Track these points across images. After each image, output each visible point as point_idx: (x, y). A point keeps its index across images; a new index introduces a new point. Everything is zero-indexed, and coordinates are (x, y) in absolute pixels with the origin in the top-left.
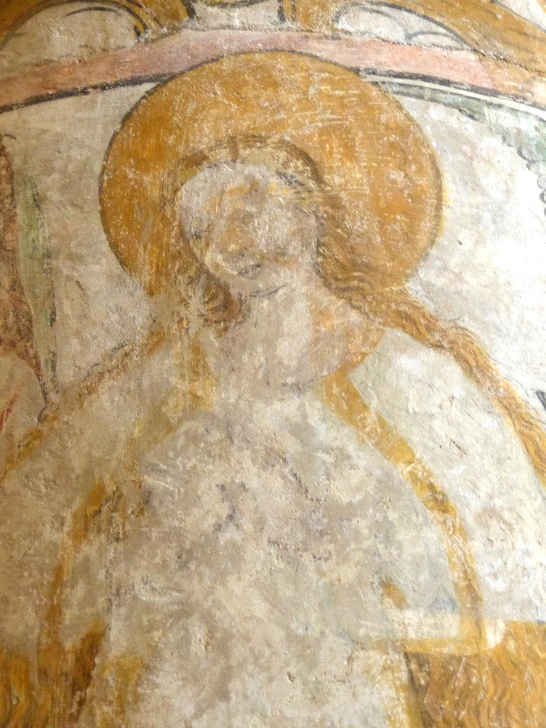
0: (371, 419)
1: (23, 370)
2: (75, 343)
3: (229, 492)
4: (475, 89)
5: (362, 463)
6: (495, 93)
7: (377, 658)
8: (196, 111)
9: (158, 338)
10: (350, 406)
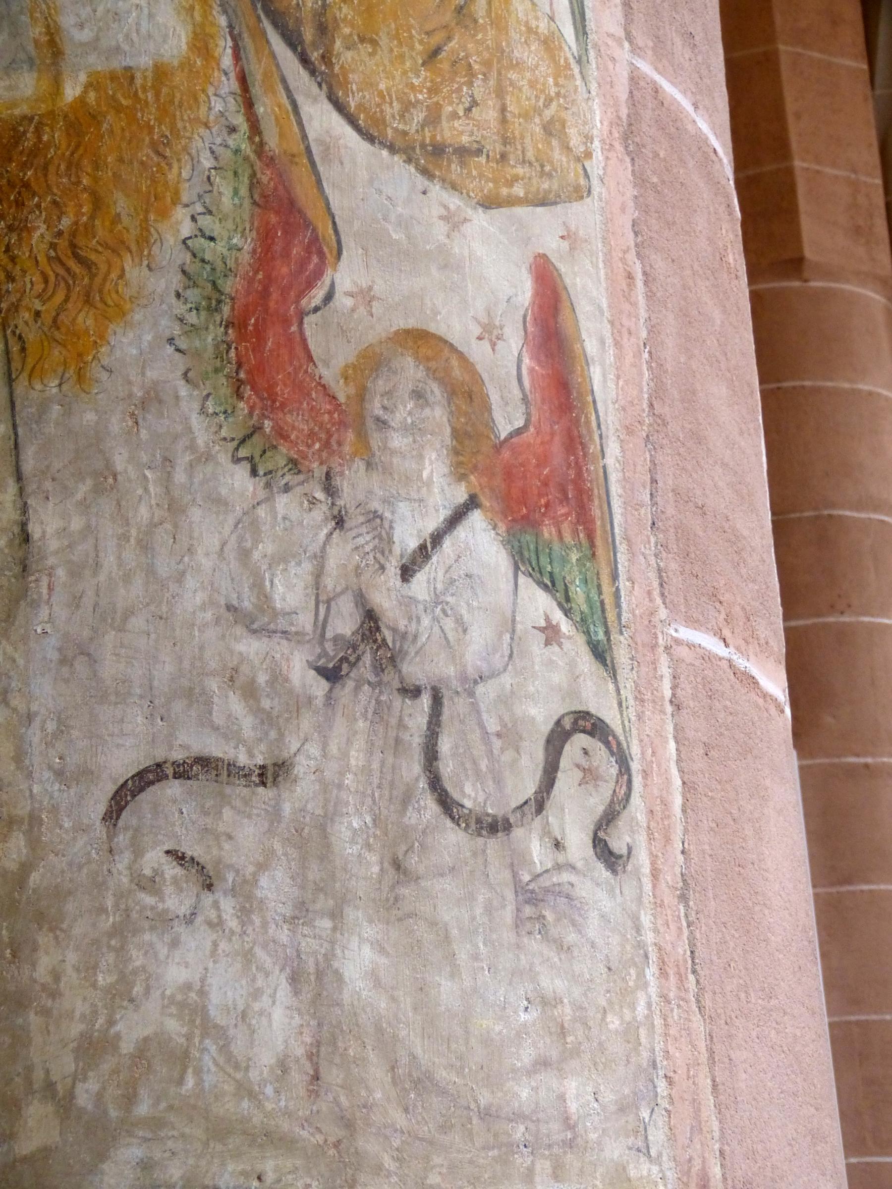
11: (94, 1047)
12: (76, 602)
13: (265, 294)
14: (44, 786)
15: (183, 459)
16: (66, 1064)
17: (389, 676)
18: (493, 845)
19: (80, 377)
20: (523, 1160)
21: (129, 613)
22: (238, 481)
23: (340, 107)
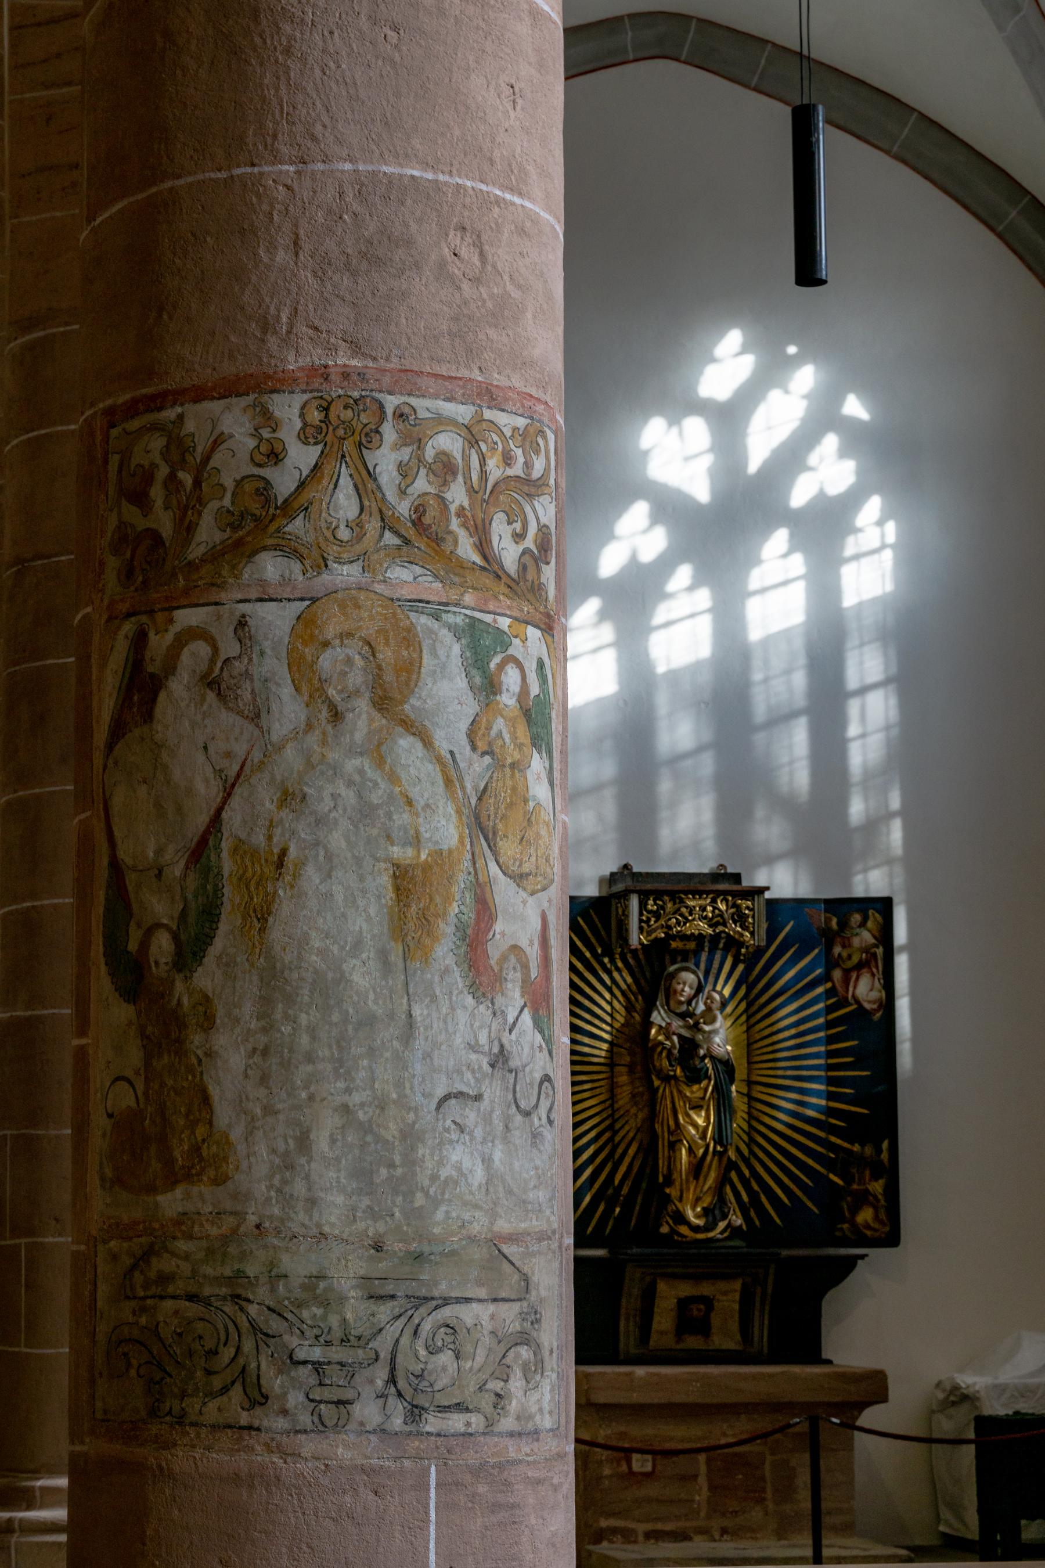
0: (387, 768)
1: (257, 732)
2: (277, 724)
3: (335, 797)
4: (440, 604)
5: (383, 787)
6: (447, 604)
7: (383, 865)
8: (327, 619)
9: (309, 727)
10: (380, 762)
11: (434, 1178)
12: (426, 1039)
13: (478, 935)
14: (419, 1098)
15: (455, 992)
16: (426, 1183)
17: (506, 1066)
18: (527, 1120)
19: (426, 962)
20: (530, 1215)
21: (441, 1044)
22: (470, 1000)
23: (498, 863)
